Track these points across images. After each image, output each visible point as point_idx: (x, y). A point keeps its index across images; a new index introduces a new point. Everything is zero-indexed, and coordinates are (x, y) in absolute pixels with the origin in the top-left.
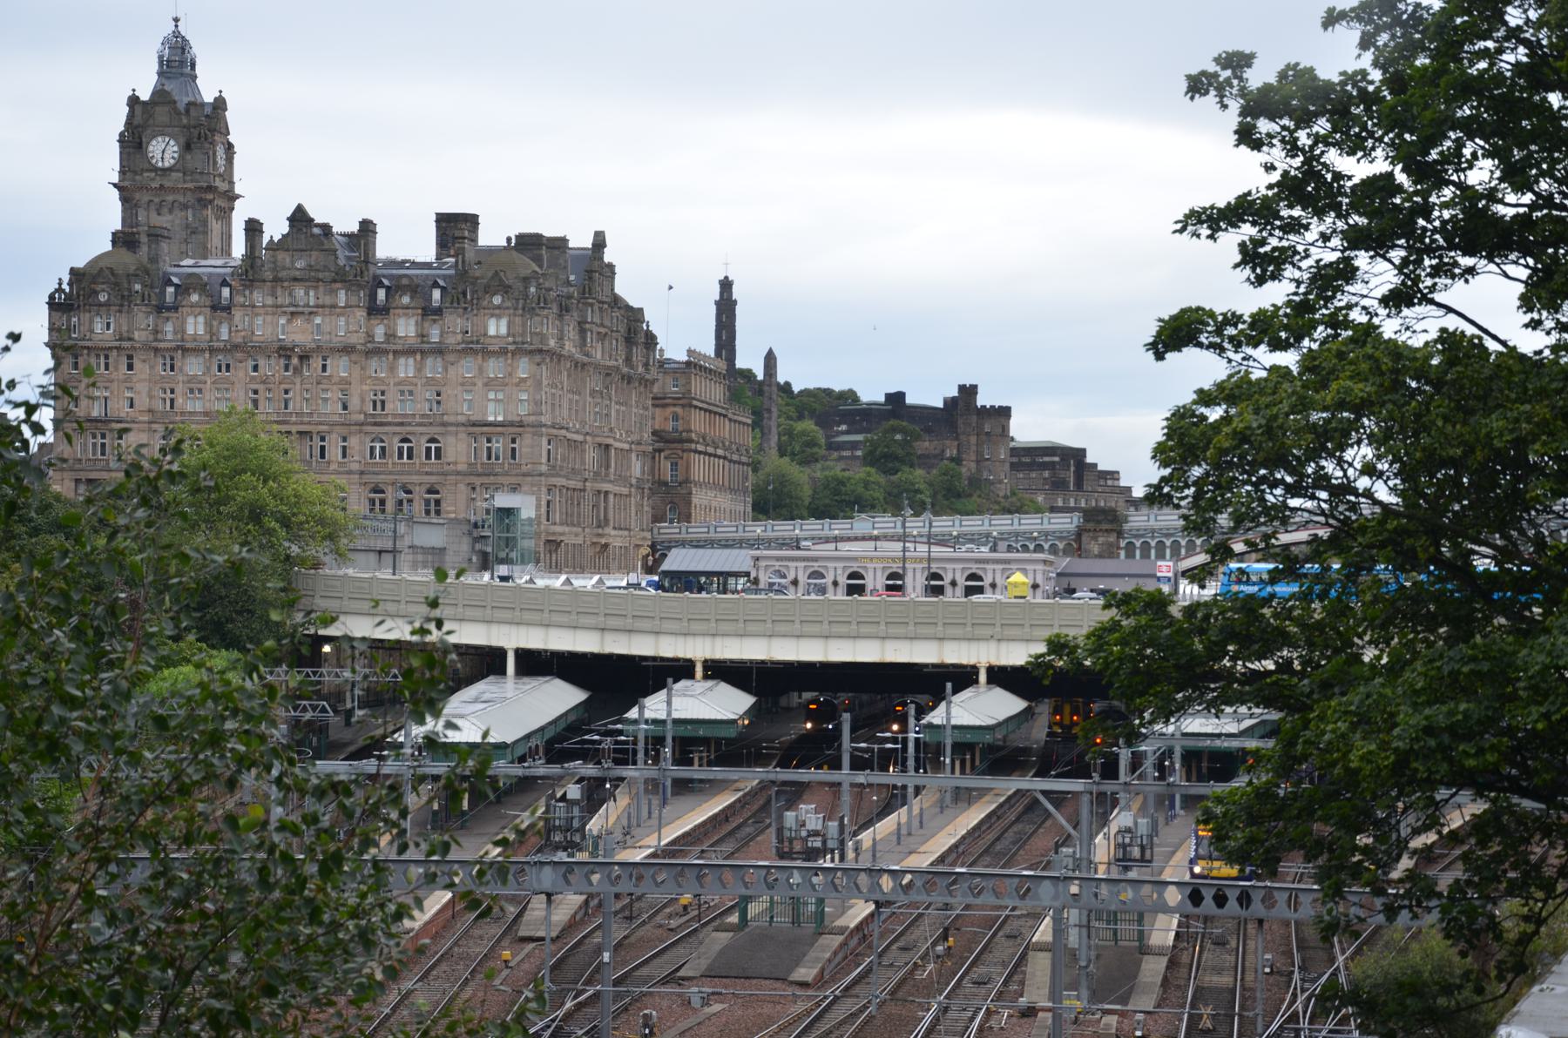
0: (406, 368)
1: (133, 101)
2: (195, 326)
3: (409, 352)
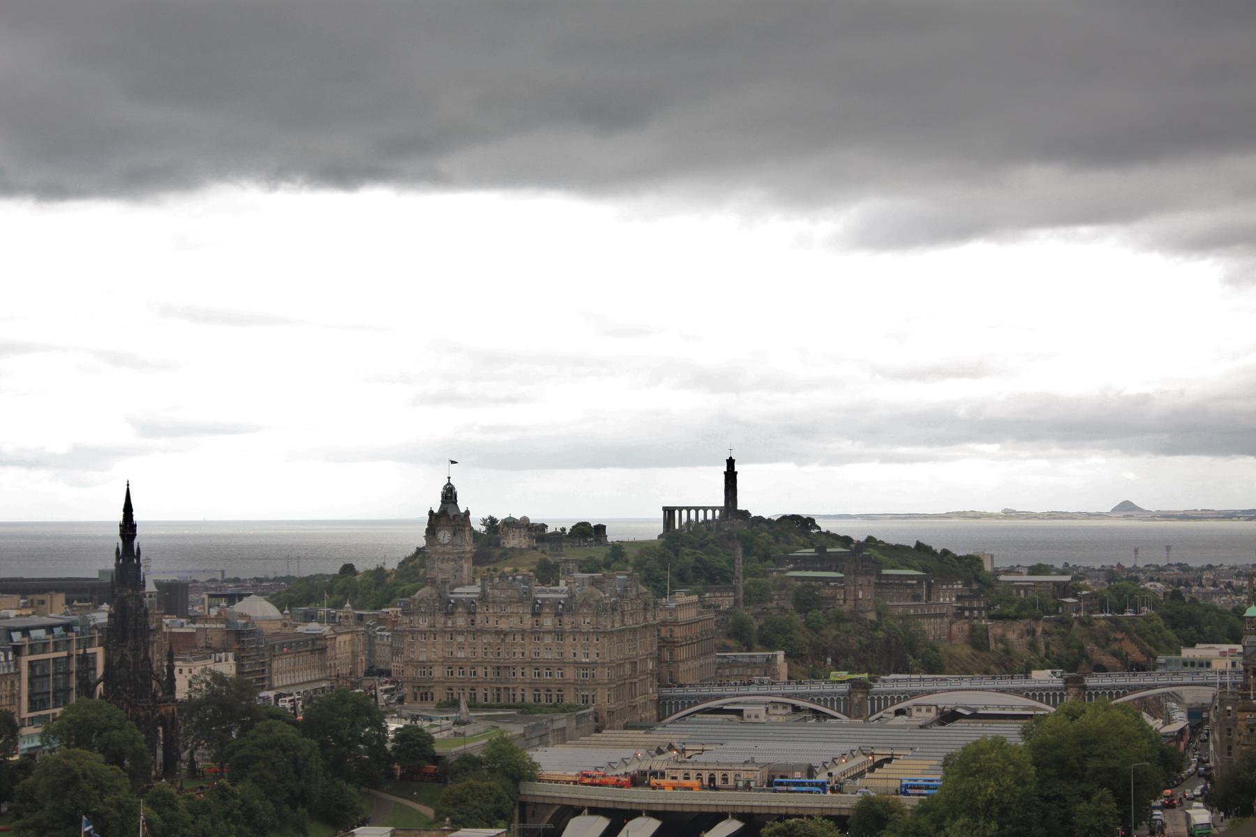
0: (548, 639)
1: (431, 513)
2: (461, 622)
3: (549, 632)
